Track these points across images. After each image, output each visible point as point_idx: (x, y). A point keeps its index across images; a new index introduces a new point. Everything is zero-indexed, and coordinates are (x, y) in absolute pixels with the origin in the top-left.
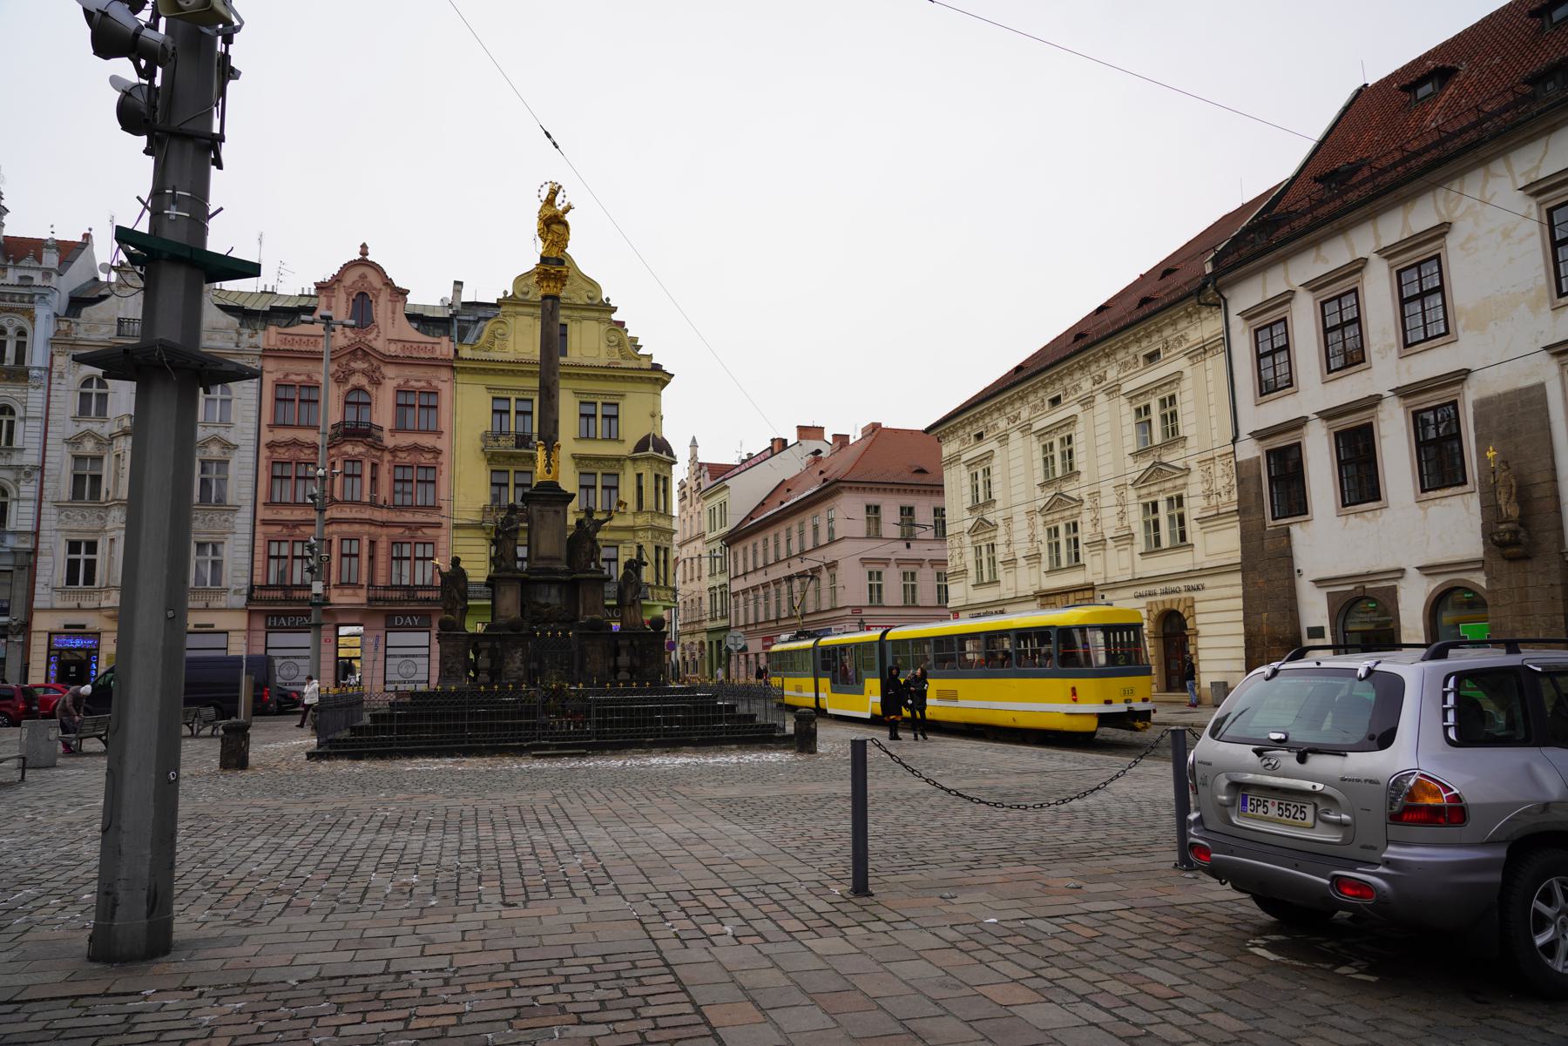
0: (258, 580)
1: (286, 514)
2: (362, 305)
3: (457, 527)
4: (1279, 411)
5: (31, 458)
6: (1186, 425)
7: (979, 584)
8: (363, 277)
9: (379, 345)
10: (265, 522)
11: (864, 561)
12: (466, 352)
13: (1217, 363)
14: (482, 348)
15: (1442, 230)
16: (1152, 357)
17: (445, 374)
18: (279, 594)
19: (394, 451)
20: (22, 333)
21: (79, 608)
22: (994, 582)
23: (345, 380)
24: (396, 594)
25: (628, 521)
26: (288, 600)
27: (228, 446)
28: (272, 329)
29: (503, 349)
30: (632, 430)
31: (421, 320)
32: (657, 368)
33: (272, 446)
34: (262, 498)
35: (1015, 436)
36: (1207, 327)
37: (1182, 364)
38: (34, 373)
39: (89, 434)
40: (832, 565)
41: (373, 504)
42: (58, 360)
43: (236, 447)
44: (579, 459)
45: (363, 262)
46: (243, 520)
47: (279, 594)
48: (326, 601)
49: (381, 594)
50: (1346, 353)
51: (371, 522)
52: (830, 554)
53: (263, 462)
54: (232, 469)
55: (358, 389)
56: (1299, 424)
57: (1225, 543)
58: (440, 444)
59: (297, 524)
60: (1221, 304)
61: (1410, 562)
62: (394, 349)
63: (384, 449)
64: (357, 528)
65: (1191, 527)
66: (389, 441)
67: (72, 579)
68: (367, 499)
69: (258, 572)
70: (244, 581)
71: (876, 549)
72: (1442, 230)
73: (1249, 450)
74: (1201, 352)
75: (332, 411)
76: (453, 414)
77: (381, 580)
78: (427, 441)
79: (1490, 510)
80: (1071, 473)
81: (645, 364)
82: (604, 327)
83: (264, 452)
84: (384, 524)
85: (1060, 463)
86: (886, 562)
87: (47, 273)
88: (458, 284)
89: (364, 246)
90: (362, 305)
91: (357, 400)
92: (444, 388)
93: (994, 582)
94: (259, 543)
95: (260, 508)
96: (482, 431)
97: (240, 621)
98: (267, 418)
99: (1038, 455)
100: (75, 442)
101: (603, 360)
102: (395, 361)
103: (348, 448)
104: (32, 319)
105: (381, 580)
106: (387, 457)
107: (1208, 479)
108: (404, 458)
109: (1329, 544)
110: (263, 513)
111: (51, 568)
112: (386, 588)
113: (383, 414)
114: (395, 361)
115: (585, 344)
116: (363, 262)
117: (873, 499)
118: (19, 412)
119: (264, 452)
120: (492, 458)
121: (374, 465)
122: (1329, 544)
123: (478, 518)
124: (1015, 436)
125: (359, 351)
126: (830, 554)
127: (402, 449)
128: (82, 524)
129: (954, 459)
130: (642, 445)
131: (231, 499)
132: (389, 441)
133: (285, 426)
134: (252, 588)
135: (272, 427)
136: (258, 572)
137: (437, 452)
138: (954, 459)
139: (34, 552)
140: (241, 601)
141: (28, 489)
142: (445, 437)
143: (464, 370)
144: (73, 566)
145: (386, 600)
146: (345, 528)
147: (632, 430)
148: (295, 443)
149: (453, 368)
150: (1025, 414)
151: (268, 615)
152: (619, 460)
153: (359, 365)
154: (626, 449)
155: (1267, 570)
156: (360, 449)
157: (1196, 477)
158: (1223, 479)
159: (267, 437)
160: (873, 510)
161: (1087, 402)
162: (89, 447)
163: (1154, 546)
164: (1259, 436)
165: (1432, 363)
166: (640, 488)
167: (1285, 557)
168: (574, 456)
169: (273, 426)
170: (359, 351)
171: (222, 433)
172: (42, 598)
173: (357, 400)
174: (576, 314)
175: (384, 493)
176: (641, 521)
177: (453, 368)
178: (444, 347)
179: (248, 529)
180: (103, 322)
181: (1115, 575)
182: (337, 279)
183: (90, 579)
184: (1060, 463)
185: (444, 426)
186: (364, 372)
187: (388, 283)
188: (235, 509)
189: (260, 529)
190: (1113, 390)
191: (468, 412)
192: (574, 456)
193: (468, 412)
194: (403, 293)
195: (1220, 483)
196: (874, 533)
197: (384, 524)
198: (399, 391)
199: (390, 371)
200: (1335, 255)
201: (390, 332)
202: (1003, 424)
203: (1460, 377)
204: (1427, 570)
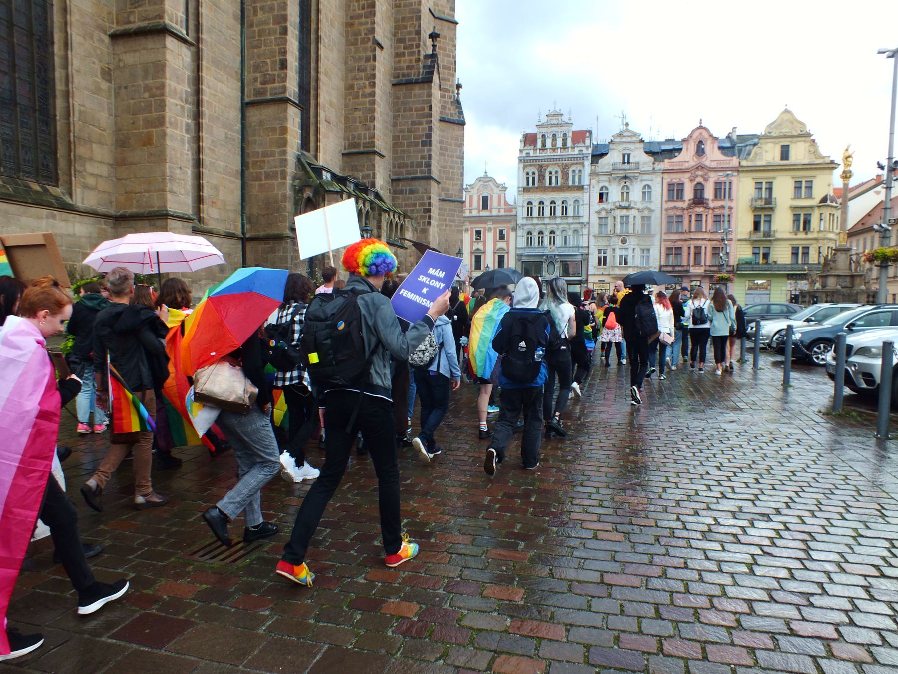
0: (662, 263)
2: (700, 152)
5: (585, 220)
8: (701, 134)
9: (707, 163)
10: (665, 240)
12: (744, 163)
19: (713, 209)
20: (580, 171)
21: (603, 274)
24: (715, 269)
27: (650, 210)
28: (666, 161)
30: (819, 192)
32: (832, 162)
33: (666, 210)
34: (663, 231)
38: (585, 187)
39: (604, 209)
42: (593, 181)
45: (701, 127)
46: (657, 238)
47: (670, 269)
48: (688, 271)
49: (708, 268)
58: (732, 204)
62: (714, 165)
64: (700, 242)
66: (712, 205)
67: (599, 263)
69: (662, 260)
75: (689, 194)
76: (738, 191)
77: (708, 263)
81: (828, 161)
82: (807, 144)
83: (664, 212)
84: (710, 240)
87: (587, 147)
90: (700, 152)
94: (663, 249)
96: (750, 197)
100: (599, 212)
101: (806, 162)
102: (714, 170)
104: (584, 166)
106: (711, 211)
108: (718, 212)
110: (664, 237)
111: (593, 260)
113: (709, 194)
114: (714, 170)
115: (799, 154)
116: (701, 127)
118: (581, 203)
120: (756, 209)
125: (701, 167)
128: (602, 243)
130: (824, 200)
131: (652, 232)
134: (660, 267)
136: (662, 260)
137: (731, 208)
139: (588, 254)
141: (585, 231)
142: (734, 201)
143: (743, 171)
144: (599, 259)
146: (696, 242)
147: (819, 192)
148: (675, 208)
149: (738, 171)
152: (811, 207)
153: (700, 173)
159: (665, 206)
162: (603, 214)
170: (701, 167)
171: (649, 206)
172: (591, 271)
174: (795, 140)
175: (709, 227)
177: (738, 171)
178: (734, 161)
179: (658, 243)
180: (608, 164)
182: (691, 136)
183: (605, 264)
185: (734, 196)
186: (702, 176)
187: (711, 136)
188: (653, 236)
191: (744, 190)
192: (791, 207)
193: (744, 190)
194: (717, 139)
197: (710, 240)
199: (712, 174)
201: (713, 156)
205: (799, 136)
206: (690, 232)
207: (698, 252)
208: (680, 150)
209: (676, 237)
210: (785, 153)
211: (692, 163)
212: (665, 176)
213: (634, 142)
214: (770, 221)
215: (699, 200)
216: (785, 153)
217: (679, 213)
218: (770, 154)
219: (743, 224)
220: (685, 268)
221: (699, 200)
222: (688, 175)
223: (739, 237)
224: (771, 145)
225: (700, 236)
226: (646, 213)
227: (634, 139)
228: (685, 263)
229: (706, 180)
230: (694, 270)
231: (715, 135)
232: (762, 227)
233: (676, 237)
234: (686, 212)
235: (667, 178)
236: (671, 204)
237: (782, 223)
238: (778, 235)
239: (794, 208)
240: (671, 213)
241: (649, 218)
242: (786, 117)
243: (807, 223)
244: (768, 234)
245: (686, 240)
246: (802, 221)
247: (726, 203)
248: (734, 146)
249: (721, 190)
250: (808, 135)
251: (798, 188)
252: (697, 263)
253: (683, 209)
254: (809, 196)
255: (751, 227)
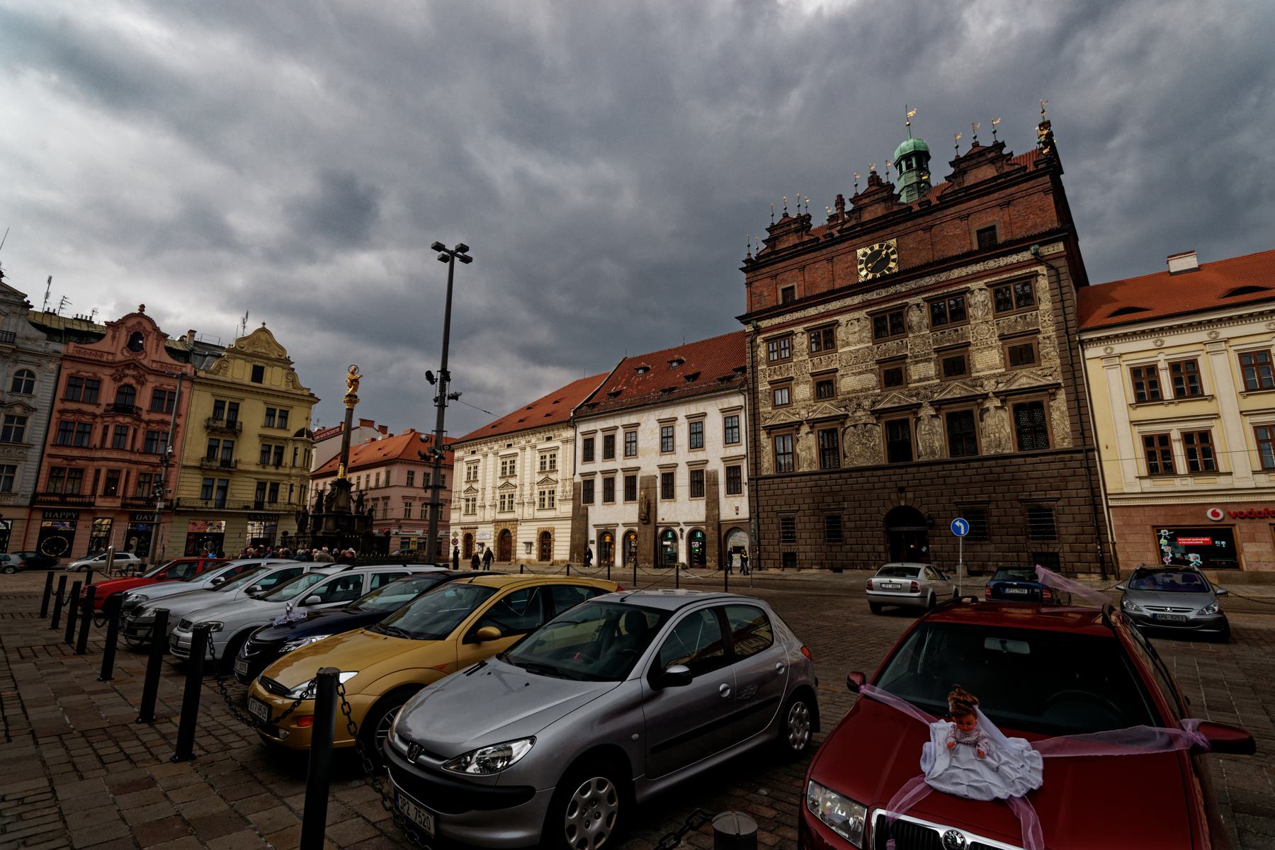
0: (40, 489)
1: (67, 452)
3: (185, 467)
4: (588, 468)
6: (559, 466)
7: (467, 514)
8: (140, 323)
9: (145, 362)
10: (50, 456)
11: (404, 497)
12: (202, 374)
13: (570, 447)
14: (211, 372)
15: (638, 425)
16: (549, 439)
17: (186, 384)
18: (57, 499)
19: (148, 422)
22: (474, 514)
23: (120, 380)
25: (287, 471)
26: (63, 502)
29: (225, 374)
31: (171, 351)
32: (312, 395)
33: (62, 412)
35: (491, 456)
36: (569, 433)
37: (559, 444)
40: (386, 498)
41: (132, 451)
43: (35, 410)
44: (262, 437)
46: (34, 453)
47: (57, 499)
48: (93, 504)
50: (609, 453)
51: (130, 462)
52: (387, 492)
53: (54, 421)
54: (29, 422)
55: (130, 386)
56: (594, 473)
57: (566, 509)
59: (74, 458)
60: (574, 427)
61: (620, 522)
62: (155, 366)
63: (142, 421)
65: (556, 502)
66: (145, 416)
68: (128, 448)
70: (30, 489)
71: (410, 492)
72: (638, 425)
73: (578, 479)
74: (566, 441)
75: (108, 394)
76: (189, 406)
77: (130, 493)
78: (171, 418)
79: (640, 508)
80: (513, 474)
81: (306, 393)
83: (56, 415)
84: (136, 463)
85: (508, 470)
86: (414, 498)
88: (192, 332)
89: (142, 307)
91: (126, 393)
92: (186, 391)
93: (474, 514)
95: (48, 446)
97: (23, 514)
98: (60, 394)
99: (500, 466)
101: (283, 388)
103: (121, 419)
105: (130, 493)
106: (143, 425)
107: (564, 486)
108: (154, 427)
109: (599, 514)
110: (49, 450)
112: (132, 499)
113: (144, 399)
115: (274, 378)
117: (412, 468)
119: (56, 415)
121: (135, 430)
122: (599, 514)
123: (198, 464)
124: (491, 456)
126: (387, 492)
127: (153, 422)
129: (461, 459)
130: (300, 433)
131: (25, 440)
132: (145, 416)
133: (72, 401)
135: (63, 400)
137: (177, 426)
138: (461, 459)
140: (27, 502)
145: (132, 506)
146: (112, 463)
147: (295, 424)
150: (496, 447)
151: (44, 511)
152: (286, 439)
154: (290, 434)
155: (580, 519)
156: (128, 420)
157: (560, 484)
158: (569, 488)
159: (59, 405)
160: (411, 474)
161: (523, 449)
163: (542, 507)
164: (582, 475)
165: (631, 463)
166: (295, 454)
167: (586, 516)
168: (260, 436)
169: (63, 400)
171: (26, 400)
173: (126, 393)
176: (294, 471)
179: (37, 459)
181: (526, 516)
182: (122, 322)
184: (508, 470)
186: (134, 377)
187: (157, 329)
188: (30, 446)
189: (46, 460)
190: (534, 447)
191: (199, 406)
192: (260, 436)
194: (165, 336)
195: (568, 489)
196: (410, 483)
198: (155, 390)
199: (151, 378)
200: (610, 423)
201: (153, 355)
202: (485, 449)
203: (638, 469)
204: (625, 525)
205: (278, 360)
206: (102, 447)
207: (113, 478)
208: (99, 337)
209: (76, 453)
210: (258, 374)
211: (119, 357)
212: (67, 364)
213: (9, 304)
214: (231, 449)
215: (124, 405)
216: (258, 374)
217: (86, 419)
218: (240, 372)
219: (194, 445)
220: (87, 500)
221: (124, 405)
222: (109, 371)
223: (185, 463)
224: (239, 363)
225: (115, 455)
226: (18, 410)
227: (11, 298)
228: (87, 490)
229: (142, 384)
230: (100, 503)
231: (163, 330)
232: (219, 454)
233: (76, 453)
234: (99, 420)
235: (69, 369)
236: (74, 406)
237: (248, 452)
238: (240, 467)
239: (262, 437)
240: (70, 417)
241: (23, 420)
242: (263, 336)
243: (280, 453)
244: (226, 463)
245: (93, 459)
246: (272, 451)
247: (171, 418)
248: (192, 351)
249: (163, 400)
250: (287, 361)
251: (270, 413)
252: (109, 493)
253: (95, 416)
254: (283, 427)
255: (202, 451)
